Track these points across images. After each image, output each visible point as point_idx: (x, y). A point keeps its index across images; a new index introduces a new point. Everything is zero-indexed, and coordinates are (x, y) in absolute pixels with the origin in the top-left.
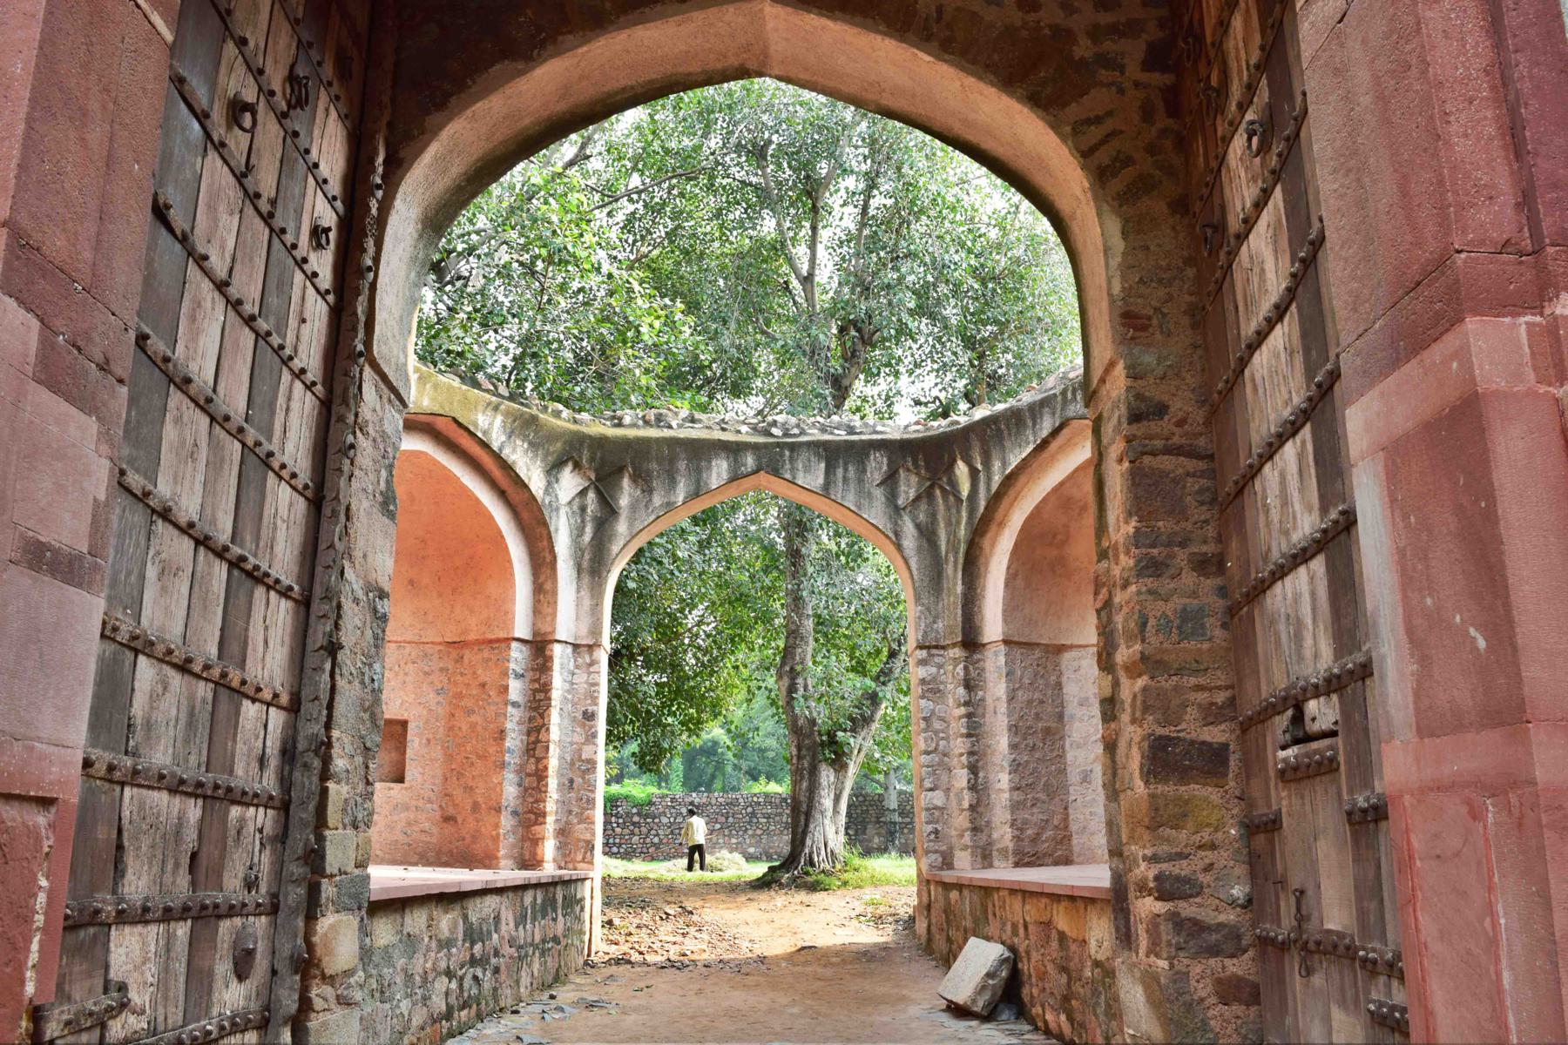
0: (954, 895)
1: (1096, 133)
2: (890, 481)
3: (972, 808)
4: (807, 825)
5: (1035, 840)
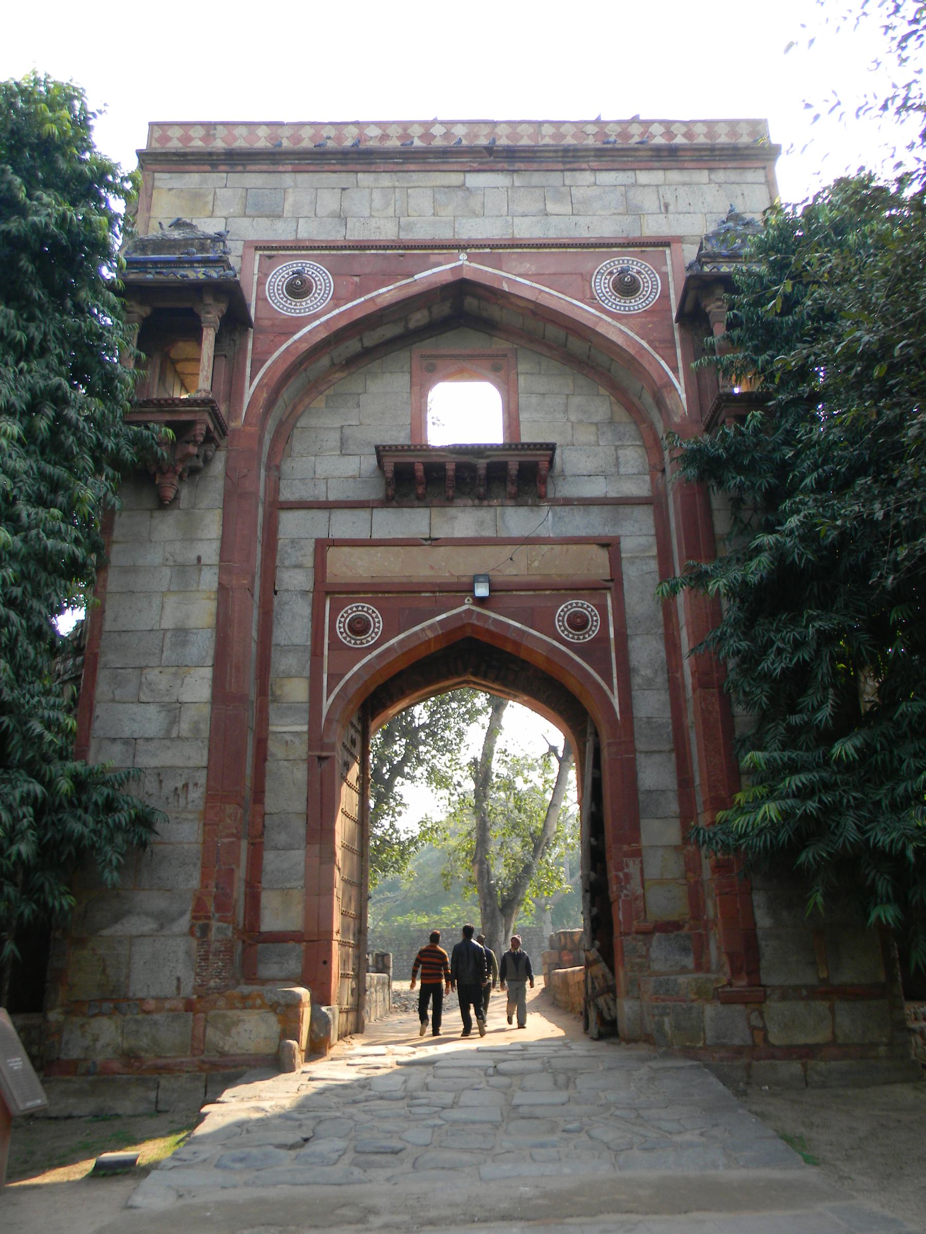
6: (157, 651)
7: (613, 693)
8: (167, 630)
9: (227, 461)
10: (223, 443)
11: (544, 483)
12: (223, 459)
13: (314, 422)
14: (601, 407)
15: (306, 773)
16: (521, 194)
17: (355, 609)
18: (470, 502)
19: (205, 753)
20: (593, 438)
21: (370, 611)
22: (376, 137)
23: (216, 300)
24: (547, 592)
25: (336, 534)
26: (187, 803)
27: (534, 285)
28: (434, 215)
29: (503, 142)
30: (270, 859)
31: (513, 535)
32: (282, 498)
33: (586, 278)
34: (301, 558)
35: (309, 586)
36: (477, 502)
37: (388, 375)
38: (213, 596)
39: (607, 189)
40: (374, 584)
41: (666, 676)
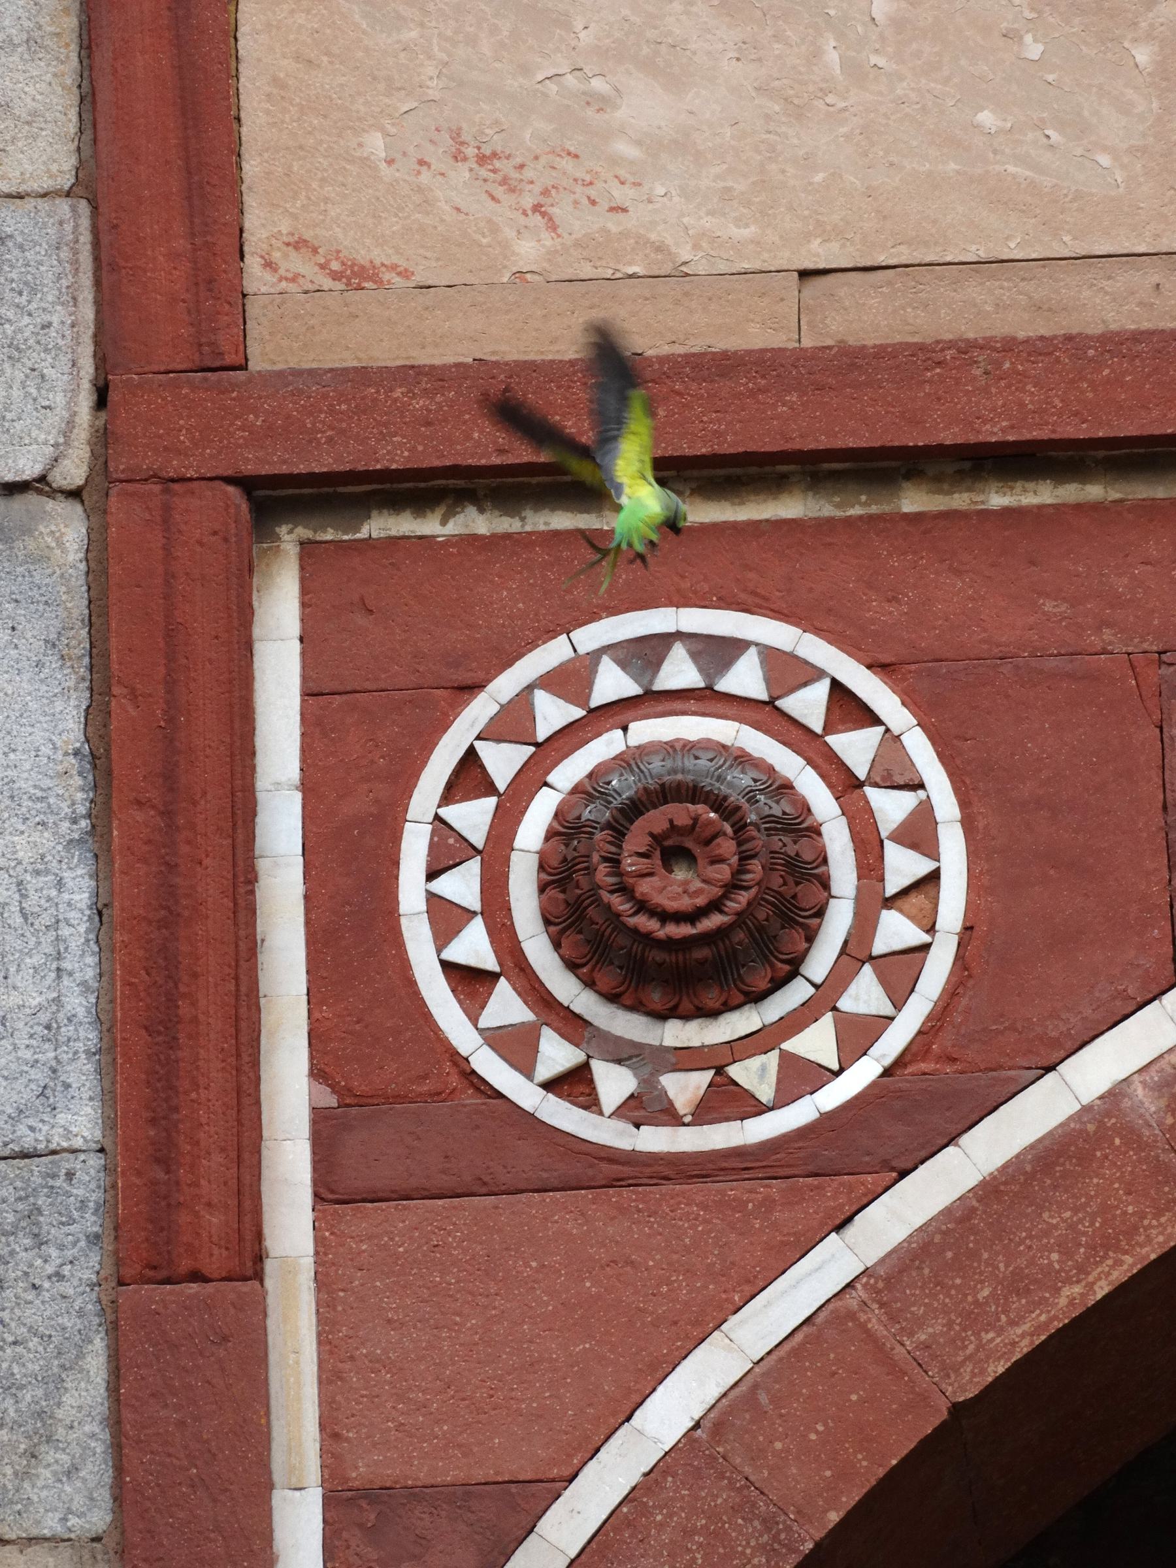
17: (613, 683)
21: (809, 704)
40: (849, 366)
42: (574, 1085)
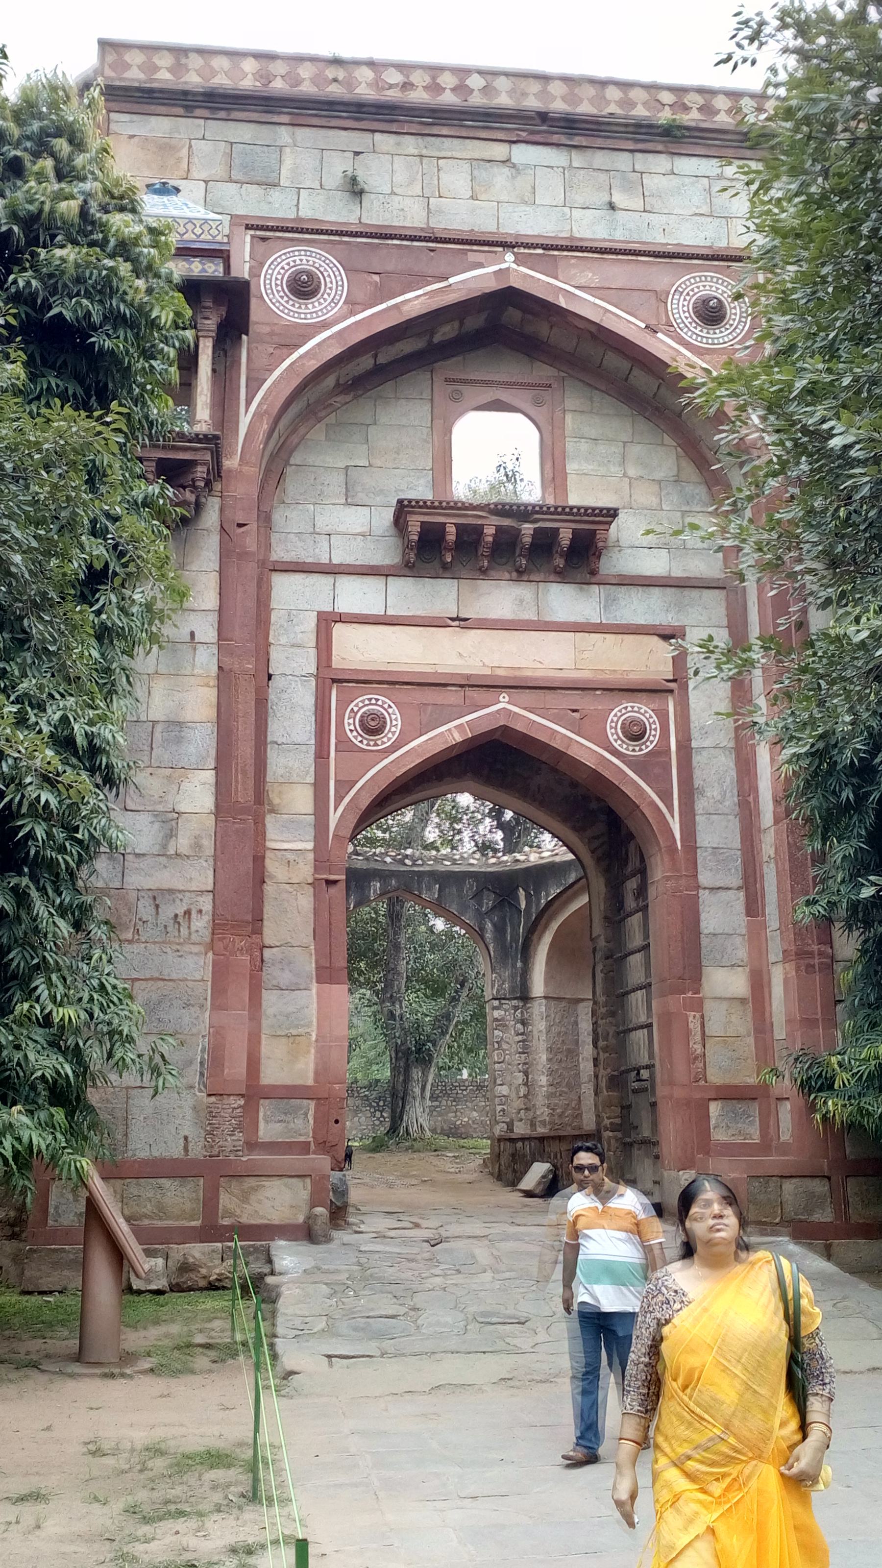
0: (519, 1144)
1: (597, 843)
2: (477, 896)
3: (525, 1096)
4: (403, 1107)
5: (560, 1116)
6: (146, 748)
7: (673, 817)
8: (155, 723)
9: (221, 510)
10: (217, 486)
11: (599, 557)
12: (217, 507)
13: (311, 460)
14: (663, 459)
15: (312, 899)
16: (581, 178)
17: (367, 702)
18: (507, 575)
19: (211, 873)
20: (654, 501)
22: (397, 85)
23: (217, 302)
24: (598, 692)
25: (344, 606)
26: (190, 934)
27: (598, 302)
28: (472, 197)
29: (558, 106)
30: (271, 1001)
31: (558, 620)
32: (274, 557)
33: (661, 298)
34: (300, 636)
35: (313, 669)
36: (514, 575)
37: (403, 402)
38: (211, 684)
39: (687, 180)
41: (736, 799)
42: (361, 742)
